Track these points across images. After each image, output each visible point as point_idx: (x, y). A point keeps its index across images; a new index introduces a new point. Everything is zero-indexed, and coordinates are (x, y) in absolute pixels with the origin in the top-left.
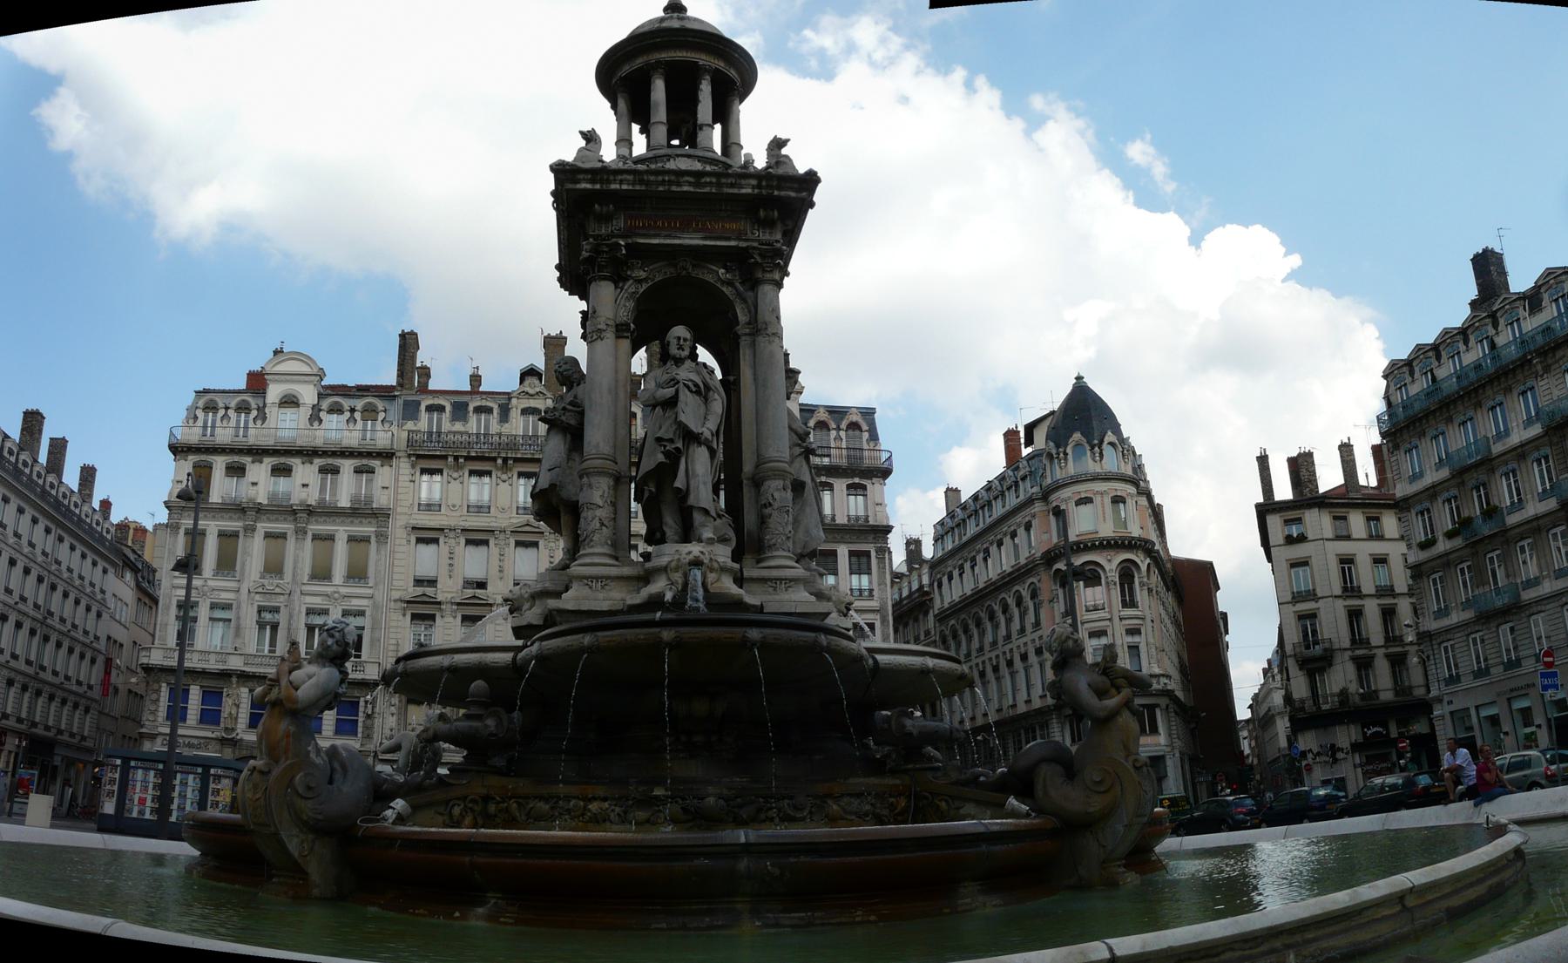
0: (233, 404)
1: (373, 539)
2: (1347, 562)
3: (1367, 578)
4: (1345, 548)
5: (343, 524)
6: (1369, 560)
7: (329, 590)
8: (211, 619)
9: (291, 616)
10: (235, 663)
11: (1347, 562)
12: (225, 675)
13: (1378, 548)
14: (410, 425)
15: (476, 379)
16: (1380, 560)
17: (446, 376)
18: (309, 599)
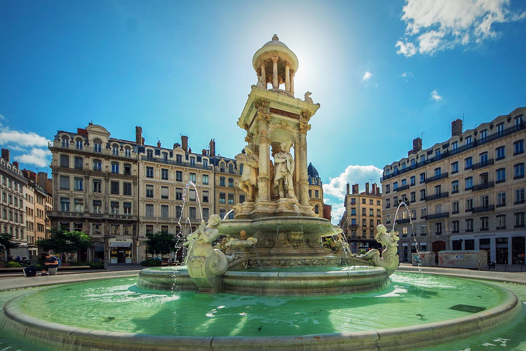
0: (75, 138)
1: (132, 184)
2: (364, 209)
3: (368, 212)
4: (364, 206)
5: (121, 179)
6: (369, 209)
7: (119, 196)
8: (75, 203)
9: (106, 203)
10: (86, 216)
11: (364, 209)
12: (83, 220)
13: (372, 207)
14: (142, 154)
15: (159, 144)
16: (371, 209)
17: (150, 141)
18: (111, 199)
